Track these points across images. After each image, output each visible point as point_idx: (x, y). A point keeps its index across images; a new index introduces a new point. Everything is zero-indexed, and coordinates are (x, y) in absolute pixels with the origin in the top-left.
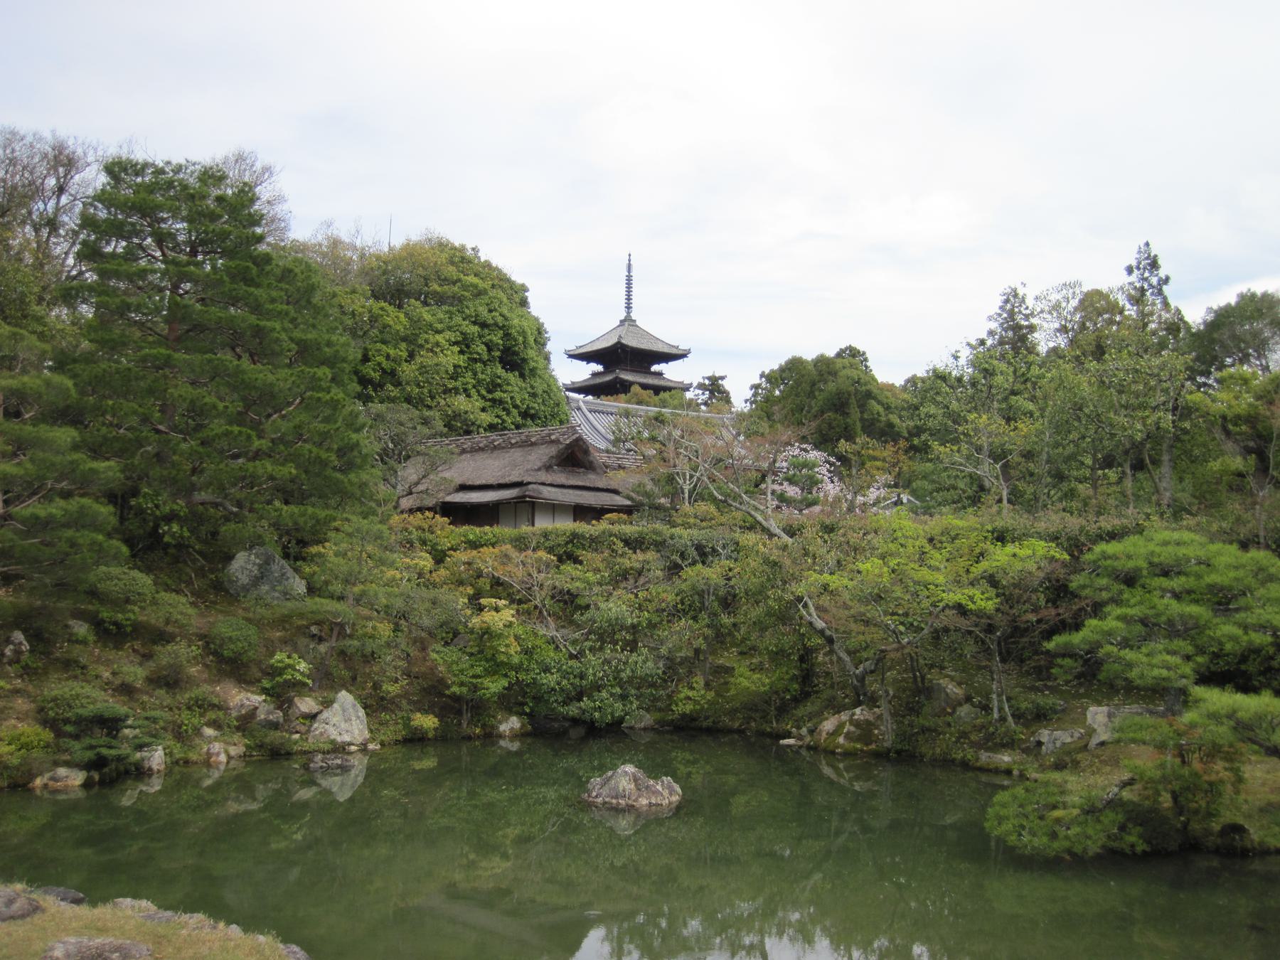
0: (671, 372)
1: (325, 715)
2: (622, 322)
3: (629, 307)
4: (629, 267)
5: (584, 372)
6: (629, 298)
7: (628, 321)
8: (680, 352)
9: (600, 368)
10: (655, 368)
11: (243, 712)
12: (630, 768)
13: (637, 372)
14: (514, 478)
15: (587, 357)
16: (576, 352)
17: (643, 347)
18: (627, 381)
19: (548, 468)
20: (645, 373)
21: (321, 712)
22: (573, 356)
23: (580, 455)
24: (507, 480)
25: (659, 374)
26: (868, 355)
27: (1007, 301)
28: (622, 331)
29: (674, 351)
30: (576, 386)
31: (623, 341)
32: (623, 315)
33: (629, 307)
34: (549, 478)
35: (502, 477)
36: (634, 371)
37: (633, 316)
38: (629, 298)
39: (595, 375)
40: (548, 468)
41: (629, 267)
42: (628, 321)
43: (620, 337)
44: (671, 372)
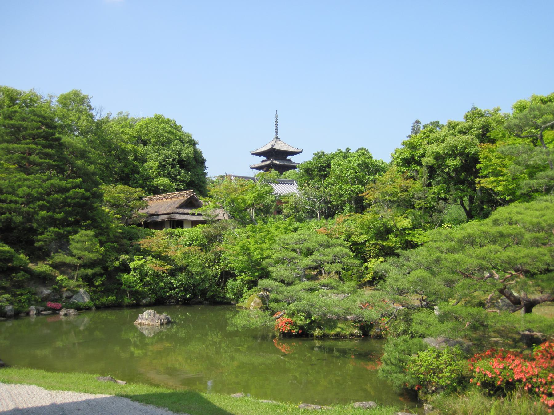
0: (295, 159)
1: (74, 297)
3: (277, 133)
5: (259, 161)
6: (277, 129)
8: (298, 151)
9: (265, 158)
10: (288, 158)
11: (45, 296)
12: (151, 310)
14: (168, 211)
18: (275, 164)
19: (181, 206)
21: (73, 296)
22: (253, 154)
23: (195, 202)
24: (165, 212)
25: (290, 160)
27: (413, 129)
28: (273, 143)
29: (296, 150)
30: (256, 166)
32: (274, 136)
33: (277, 133)
34: (181, 211)
35: (165, 210)
36: (278, 159)
38: (277, 129)
39: (263, 161)
40: (181, 206)
44: (295, 159)
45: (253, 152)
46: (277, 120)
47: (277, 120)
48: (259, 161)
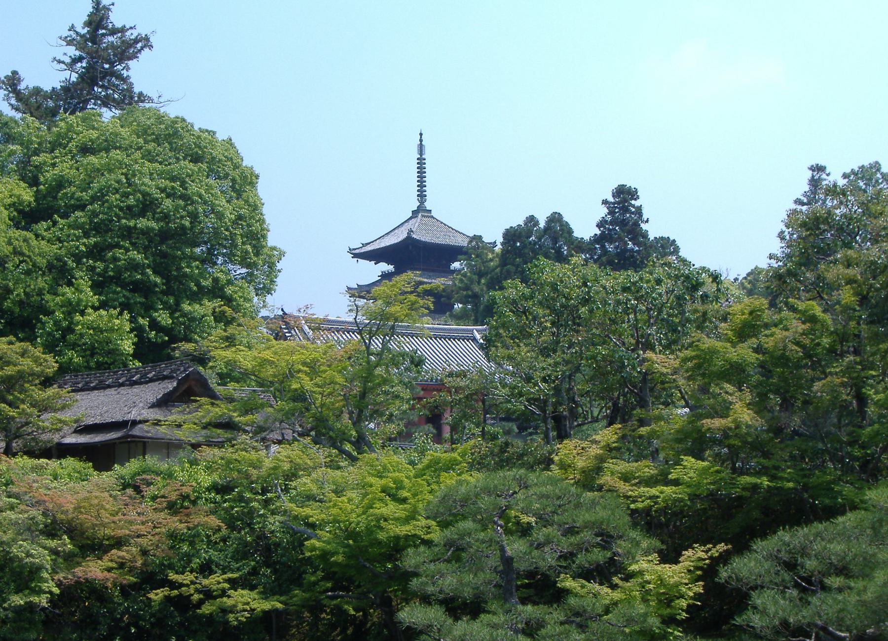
2: (415, 213)
3: (422, 196)
4: (421, 148)
7: (421, 211)
13: (433, 271)
15: (375, 256)
16: (363, 250)
17: (438, 241)
20: (444, 272)
22: (356, 256)
26: (678, 243)
31: (414, 236)
32: (415, 205)
33: (422, 196)
37: (428, 205)
41: (421, 148)
42: (421, 211)
43: (411, 231)
45: (357, 251)
46: (421, 162)
47: (421, 162)
48: (372, 271)
